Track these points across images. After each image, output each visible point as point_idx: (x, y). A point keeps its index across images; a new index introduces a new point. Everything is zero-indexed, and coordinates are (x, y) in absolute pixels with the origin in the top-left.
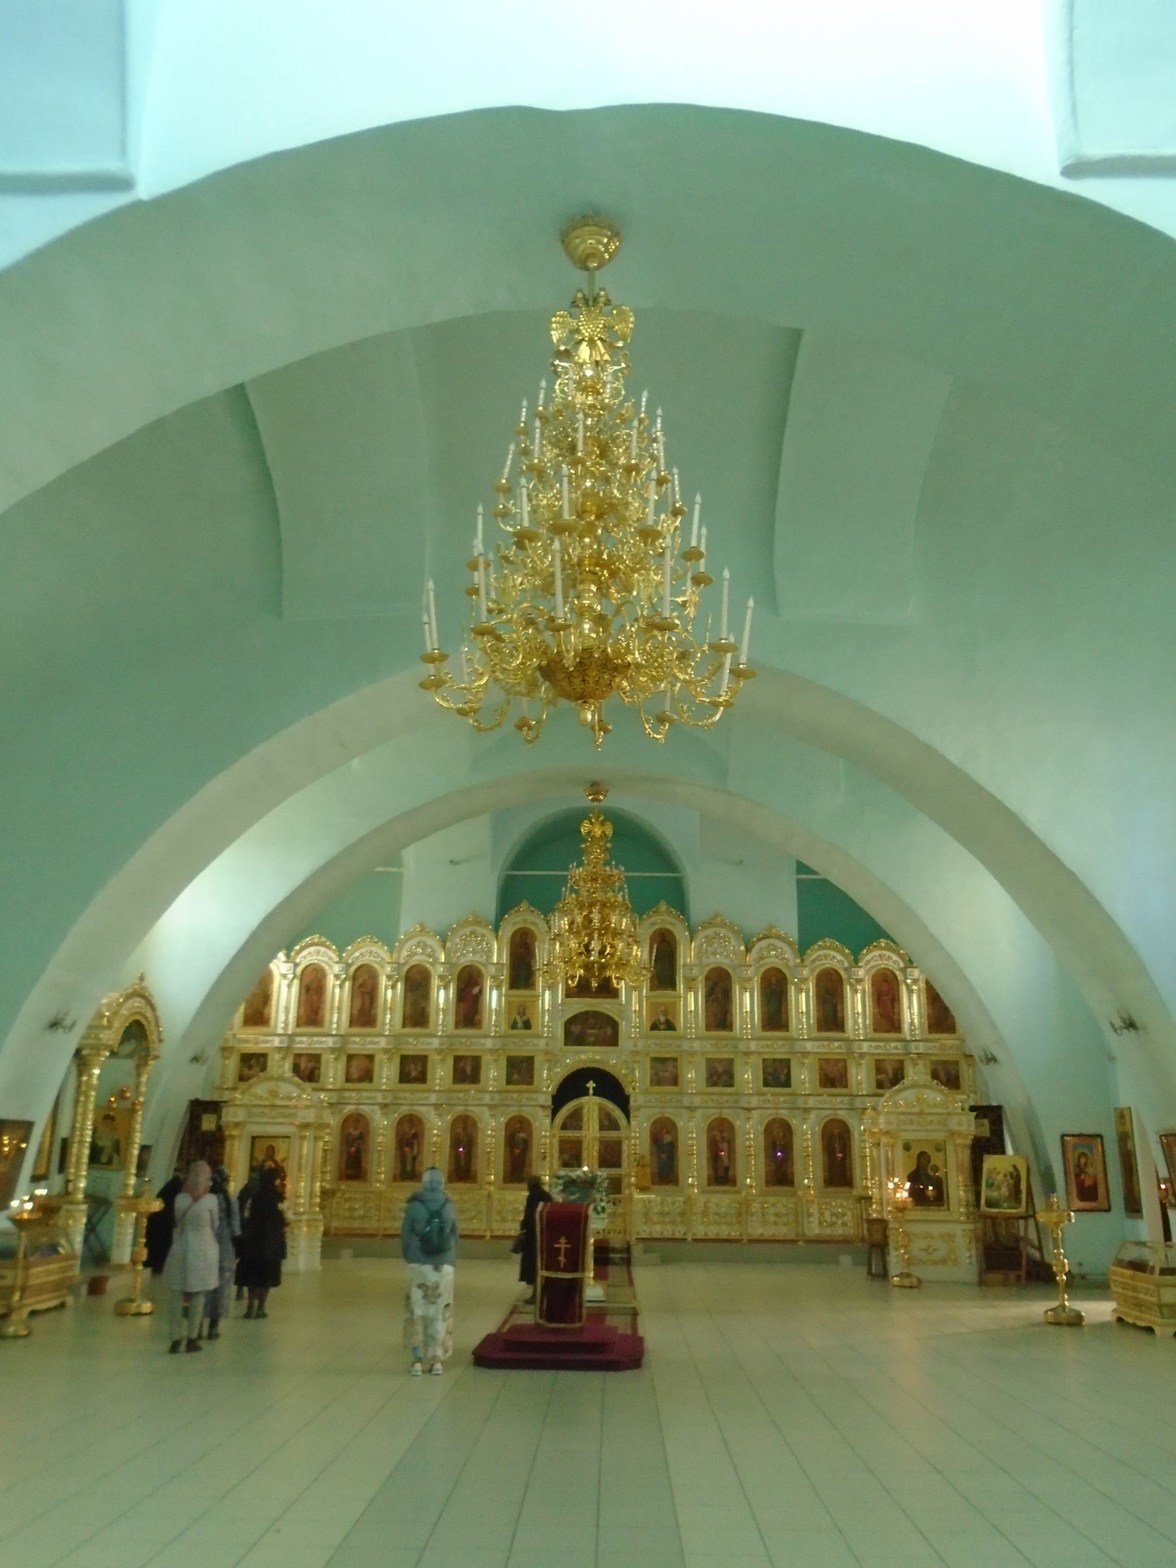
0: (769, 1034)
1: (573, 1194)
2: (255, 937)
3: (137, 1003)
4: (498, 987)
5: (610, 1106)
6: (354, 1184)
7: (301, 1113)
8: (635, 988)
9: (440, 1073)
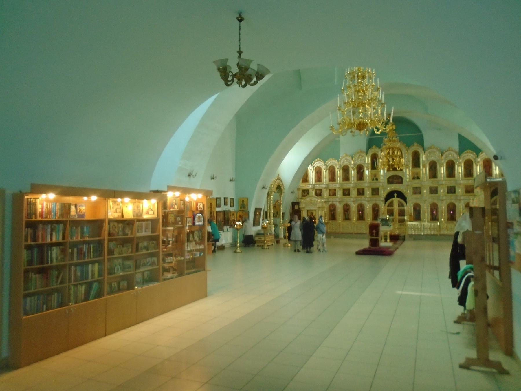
0: (448, 179)
2: (303, 163)
3: (279, 181)
4: (368, 169)
5: (401, 200)
9: (354, 193)
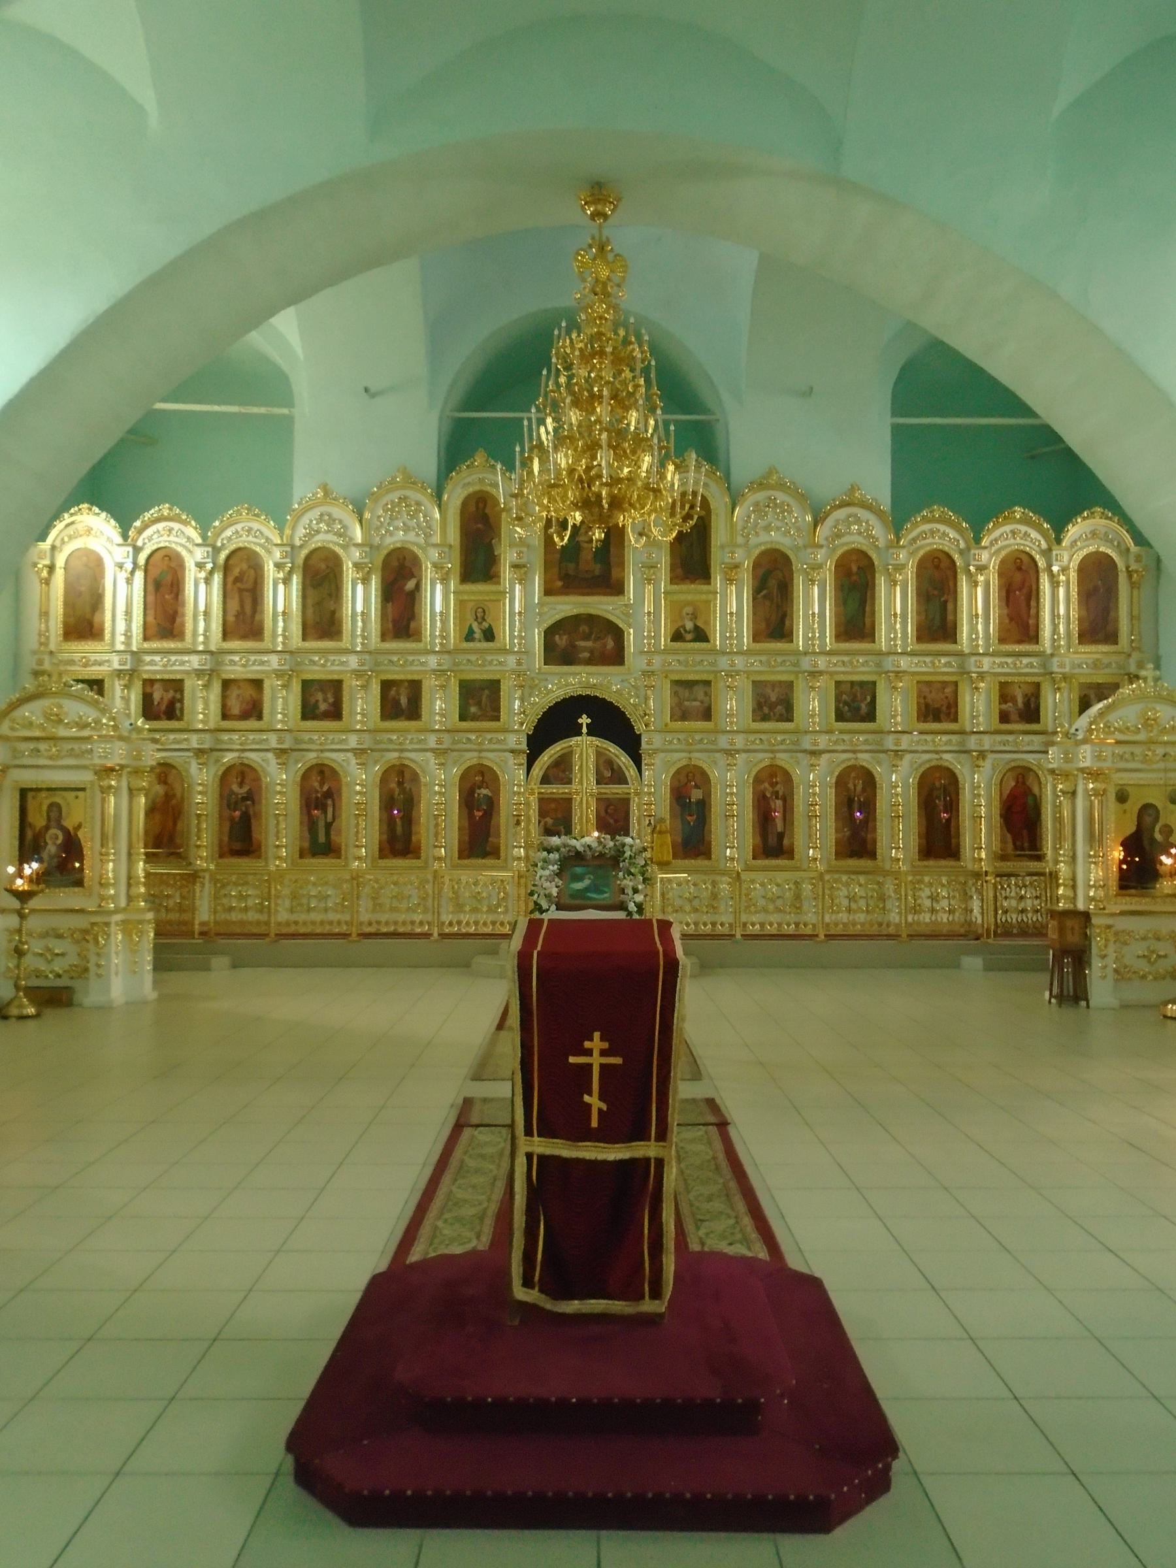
1: (579, 878)
4: (444, 580)
5: (613, 749)
6: (244, 863)
7: (100, 749)
8: (649, 581)
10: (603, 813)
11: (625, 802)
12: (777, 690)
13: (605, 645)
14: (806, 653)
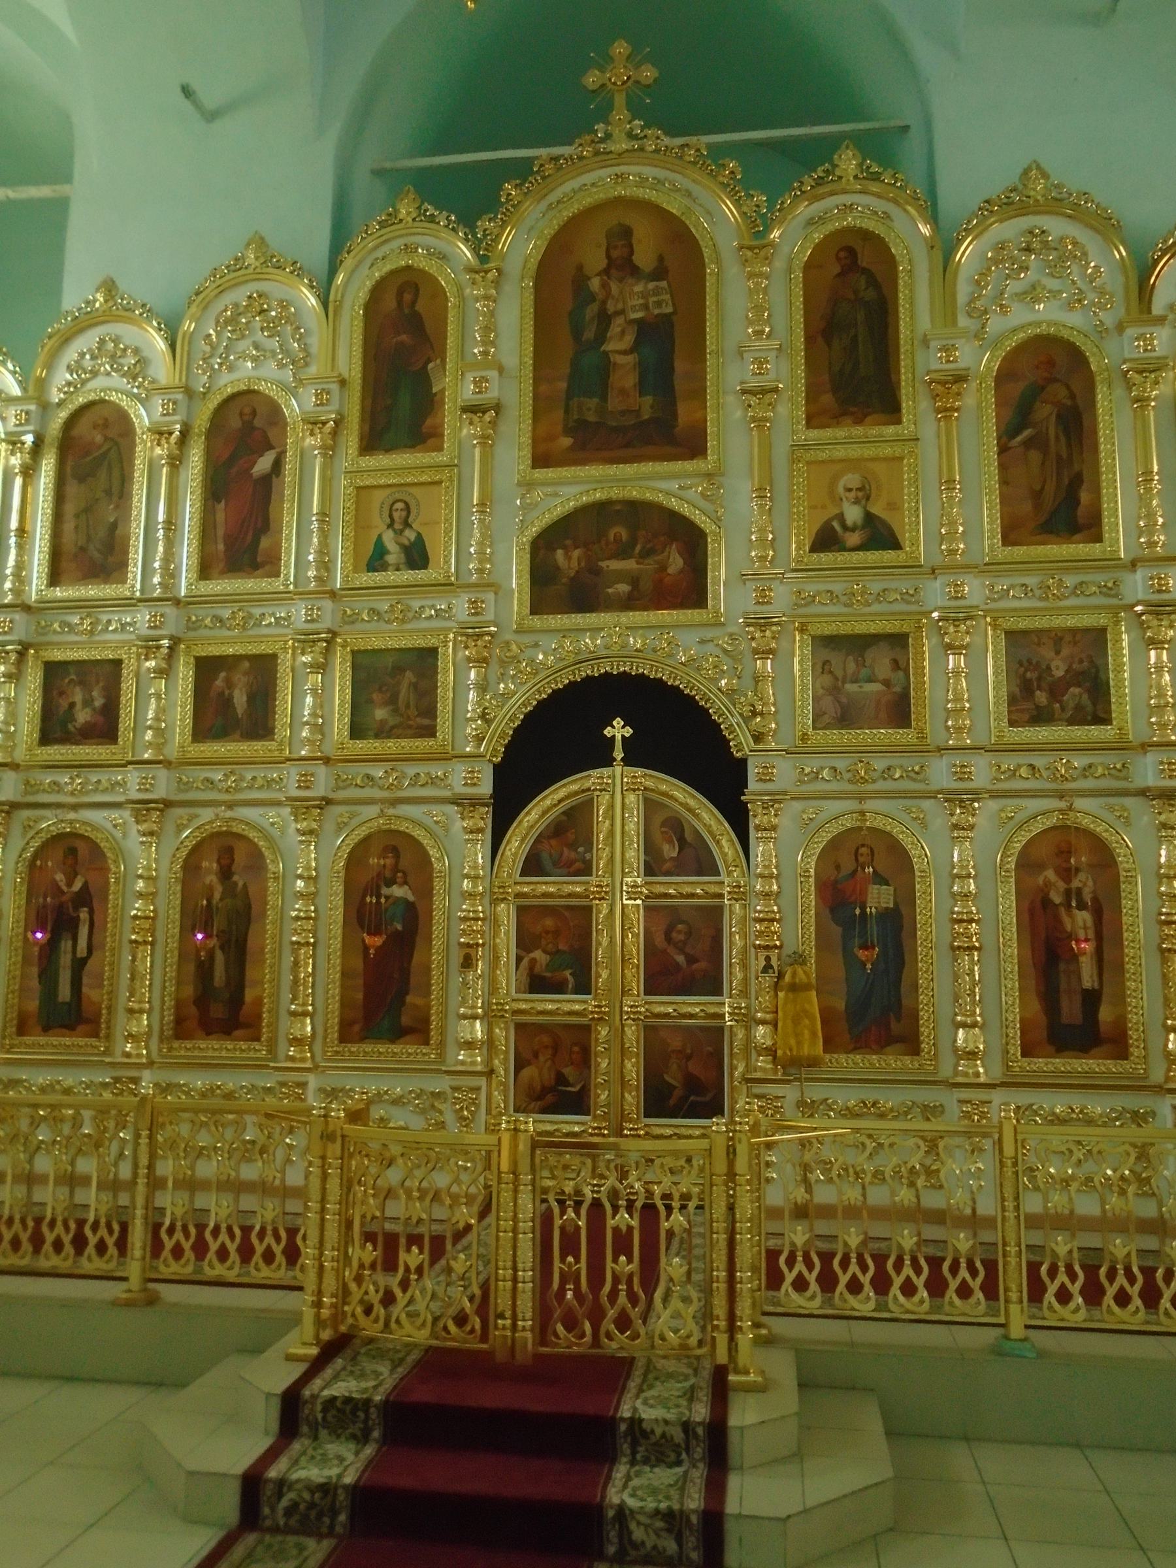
5: (682, 795)
10: (660, 940)
11: (713, 914)
12: (1065, 652)
13: (663, 568)
14: (1133, 565)
